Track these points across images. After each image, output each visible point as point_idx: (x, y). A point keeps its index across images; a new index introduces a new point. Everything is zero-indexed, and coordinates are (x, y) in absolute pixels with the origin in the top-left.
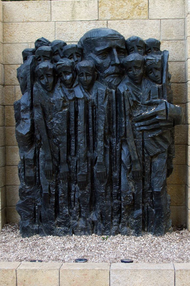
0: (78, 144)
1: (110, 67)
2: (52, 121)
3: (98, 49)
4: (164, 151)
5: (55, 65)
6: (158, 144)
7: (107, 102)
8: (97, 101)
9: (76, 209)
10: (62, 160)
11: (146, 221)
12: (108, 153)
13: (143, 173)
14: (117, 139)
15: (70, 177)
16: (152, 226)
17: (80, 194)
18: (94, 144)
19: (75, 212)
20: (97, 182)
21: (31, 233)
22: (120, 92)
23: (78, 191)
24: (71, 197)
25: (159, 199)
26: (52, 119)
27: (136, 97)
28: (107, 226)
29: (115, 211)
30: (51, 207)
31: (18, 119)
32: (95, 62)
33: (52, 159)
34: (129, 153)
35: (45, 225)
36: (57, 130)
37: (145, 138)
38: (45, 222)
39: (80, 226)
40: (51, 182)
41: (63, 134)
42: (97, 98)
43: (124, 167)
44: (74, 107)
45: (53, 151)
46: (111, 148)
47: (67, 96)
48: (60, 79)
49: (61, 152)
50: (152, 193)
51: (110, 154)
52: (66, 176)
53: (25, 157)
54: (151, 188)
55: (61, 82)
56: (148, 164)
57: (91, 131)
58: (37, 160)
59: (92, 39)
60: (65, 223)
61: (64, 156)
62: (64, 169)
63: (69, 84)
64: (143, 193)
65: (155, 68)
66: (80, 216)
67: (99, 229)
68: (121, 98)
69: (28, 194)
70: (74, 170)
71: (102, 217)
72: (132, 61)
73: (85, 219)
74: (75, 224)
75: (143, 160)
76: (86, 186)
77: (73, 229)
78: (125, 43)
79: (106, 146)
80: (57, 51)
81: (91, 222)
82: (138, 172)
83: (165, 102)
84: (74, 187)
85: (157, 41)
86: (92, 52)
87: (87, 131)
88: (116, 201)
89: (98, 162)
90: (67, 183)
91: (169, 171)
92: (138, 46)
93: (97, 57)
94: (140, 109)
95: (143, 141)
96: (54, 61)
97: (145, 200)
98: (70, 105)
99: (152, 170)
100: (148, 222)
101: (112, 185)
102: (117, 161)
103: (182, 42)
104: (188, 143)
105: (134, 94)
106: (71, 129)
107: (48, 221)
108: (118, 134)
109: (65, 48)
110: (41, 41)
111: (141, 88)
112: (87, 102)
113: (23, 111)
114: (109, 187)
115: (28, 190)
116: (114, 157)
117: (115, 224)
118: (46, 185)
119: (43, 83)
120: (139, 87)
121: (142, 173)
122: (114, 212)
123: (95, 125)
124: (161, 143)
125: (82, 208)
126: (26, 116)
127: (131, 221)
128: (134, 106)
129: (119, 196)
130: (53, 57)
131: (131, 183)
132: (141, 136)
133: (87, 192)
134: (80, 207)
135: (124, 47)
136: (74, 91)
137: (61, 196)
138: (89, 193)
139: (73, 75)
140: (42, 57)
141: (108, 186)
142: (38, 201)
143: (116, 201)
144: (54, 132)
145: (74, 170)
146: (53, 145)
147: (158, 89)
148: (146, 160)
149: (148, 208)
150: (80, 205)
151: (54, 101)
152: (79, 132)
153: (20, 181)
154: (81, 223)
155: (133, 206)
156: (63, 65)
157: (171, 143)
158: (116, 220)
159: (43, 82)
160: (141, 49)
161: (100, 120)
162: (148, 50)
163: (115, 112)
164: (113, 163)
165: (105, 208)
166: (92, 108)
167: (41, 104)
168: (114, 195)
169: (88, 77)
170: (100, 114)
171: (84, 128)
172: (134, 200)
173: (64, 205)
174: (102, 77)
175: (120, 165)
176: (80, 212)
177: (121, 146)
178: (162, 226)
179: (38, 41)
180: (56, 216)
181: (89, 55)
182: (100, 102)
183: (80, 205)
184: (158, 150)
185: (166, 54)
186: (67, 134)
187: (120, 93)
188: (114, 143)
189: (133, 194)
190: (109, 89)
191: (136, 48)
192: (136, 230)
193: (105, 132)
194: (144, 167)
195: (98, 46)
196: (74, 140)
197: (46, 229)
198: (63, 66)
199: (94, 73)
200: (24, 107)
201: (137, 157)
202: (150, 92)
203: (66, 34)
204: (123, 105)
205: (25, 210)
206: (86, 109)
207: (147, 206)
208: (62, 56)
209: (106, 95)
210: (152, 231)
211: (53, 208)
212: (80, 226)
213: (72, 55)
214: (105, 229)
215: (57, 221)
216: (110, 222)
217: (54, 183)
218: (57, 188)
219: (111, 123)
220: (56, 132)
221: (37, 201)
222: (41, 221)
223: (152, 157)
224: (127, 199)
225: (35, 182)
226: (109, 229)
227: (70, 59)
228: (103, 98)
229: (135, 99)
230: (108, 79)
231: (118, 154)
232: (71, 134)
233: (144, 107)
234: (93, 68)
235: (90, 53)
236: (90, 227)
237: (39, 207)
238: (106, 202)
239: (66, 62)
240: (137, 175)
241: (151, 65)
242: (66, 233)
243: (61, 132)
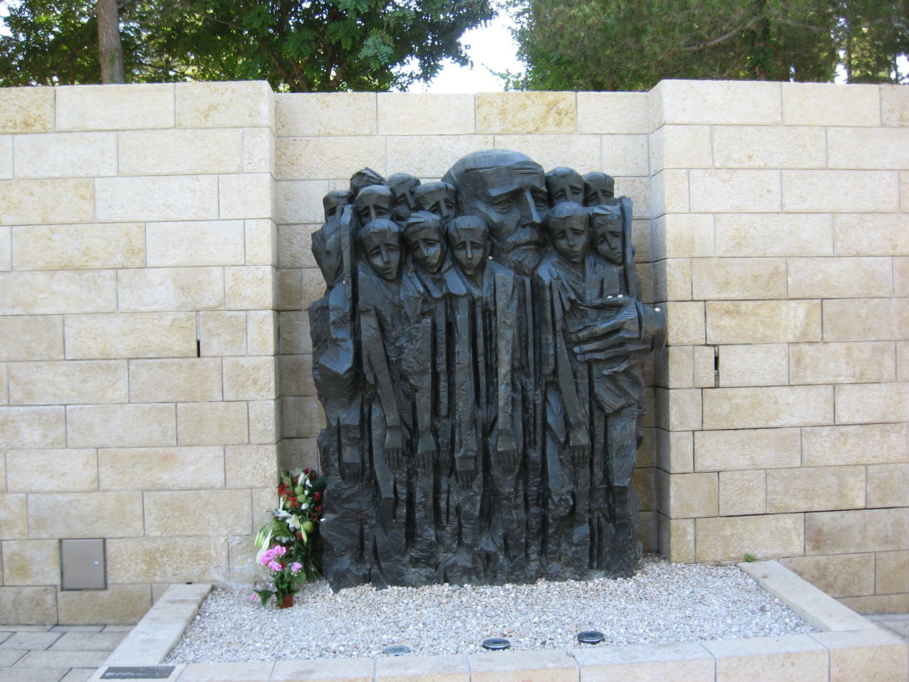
3: (494, 192)
6: (621, 389)
7: (515, 302)
20: (496, 472)
22: (543, 282)
38: (386, 560)
43: (552, 437)
46: (524, 399)
49: (419, 409)
52: (431, 459)
57: (482, 366)
60: (429, 558)
61: (425, 418)
62: (425, 445)
63: (432, 266)
64: (590, 489)
74: (451, 561)
79: (515, 396)
81: (484, 555)
111: (584, 273)
113: (333, 323)
117: (534, 556)
126: (343, 334)
132: (586, 373)
136: (444, 280)
137: (421, 503)
154: (463, 559)
155: (572, 518)
159: (378, 261)
164: (529, 431)
167: (376, 309)
175: (544, 435)
182: (500, 305)
184: (622, 402)
194: (592, 436)
195: (493, 187)
198: (423, 229)
204: (549, 308)
207: (599, 518)
213: (437, 204)
217: (404, 475)
220: (409, 367)
225: (363, 474)
226: (523, 568)
227: (434, 212)
229: (573, 297)
237: (372, 527)
242: (430, 581)
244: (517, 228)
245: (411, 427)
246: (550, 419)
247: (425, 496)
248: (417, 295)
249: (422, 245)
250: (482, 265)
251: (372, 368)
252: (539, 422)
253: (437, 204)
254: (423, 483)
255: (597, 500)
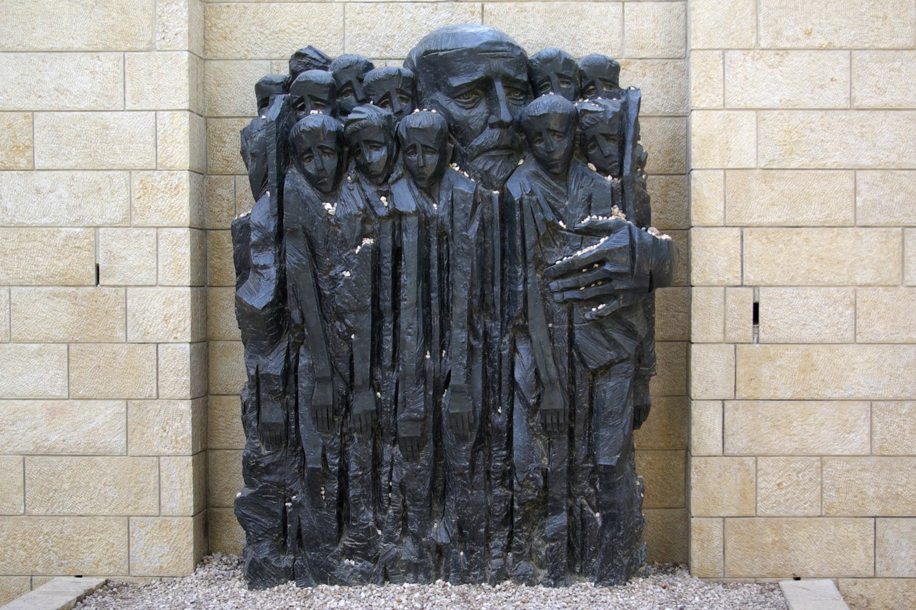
0: (402, 336)
1: (488, 130)
2: (332, 273)
3: (456, 82)
4: (625, 356)
5: (343, 122)
6: (610, 340)
7: (476, 224)
8: (452, 222)
9: (394, 513)
10: (358, 381)
11: (578, 546)
12: (480, 359)
13: (570, 416)
14: (502, 323)
15: (379, 425)
16: (594, 560)
17: (404, 472)
18: (442, 336)
19: (390, 521)
20: (449, 439)
21: (274, 576)
22: (513, 198)
23: (400, 463)
24: (380, 479)
25: (608, 487)
26: (332, 267)
27: (554, 210)
28: (476, 559)
29: (497, 519)
30: (328, 506)
31: (244, 268)
32: (448, 115)
33: (332, 376)
34: (535, 362)
35: (310, 555)
36: (346, 297)
37: (575, 320)
38: (311, 549)
39: (403, 558)
40: (328, 438)
41: (361, 310)
42: (451, 214)
44: (390, 237)
45: (334, 355)
46: (488, 347)
47: (372, 207)
48: (356, 160)
50: (595, 470)
51: (484, 364)
52: (369, 422)
54: (591, 455)
55: (356, 168)
56: (584, 392)
57: (435, 303)
58: (292, 378)
59: (441, 54)
60: (365, 549)
61: (362, 368)
62: (362, 403)
63: (377, 176)
64: (569, 468)
65: (604, 135)
66: (405, 532)
67: (455, 567)
68: (515, 214)
69: (267, 470)
70: (391, 407)
71: (465, 533)
72: (544, 115)
73: (416, 538)
75: (572, 381)
76: (420, 450)
77: (386, 566)
78: (528, 66)
79: (474, 343)
80: (349, 83)
81: (434, 548)
82: (557, 412)
83: (629, 225)
84: (390, 451)
85: (611, 61)
86: (440, 90)
87: (426, 303)
88: (498, 492)
89: (454, 386)
90: (370, 443)
91: (640, 415)
92: (560, 76)
93: (453, 104)
94: (565, 245)
95: (571, 331)
96: (339, 112)
97: (576, 489)
98: (379, 230)
99: (595, 408)
100: (582, 549)
101: (490, 449)
102: (503, 383)
103: (679, 63)
104: (690, 337)
105: (549, 203)
106: (382, 297)
107: (318, 544)
108: (507, 311)
109: (369, 77)
110: (305, 55)
111: (567, 187)
112: (425, 221)
113: (255, 245)
114: (481, 453)
115: (267, 461)
116: (494, 373)
117: (496, 552)
118: (316, 446)
119: (310, 171)
120: (560, 186)
121: (568, 414)
122: (495, 522)
123: (445, 285)
124: (616, 336)
125: (409, 511)
126: (265, 258)
127: (539, 546)
128: (548, 236)
129: (507, 475)
130: (338, 100)
131: (539, 442)
132: (565, 317)
133: (422, 465)
134: (405, 507)
135: (524, 78)
136: (392, 194)
137: (356, 477)
138: (428, 470)
139: (390, 151)
140: (307, 99)
141: (479, 450)
142: (295, 490)
143: (498, 492)
144: (339, 304)
145: (391, 407)
146: (334, 337)
147: (610, 192)
148: (578, 382)
149: (582, 511)
150: (404, 501)
151: (338, 219)
152: (402, 303)
153: (247, 437)
154: (407, 550)
155: (545, 505)
156: (363, 122)
157: (644, 336)
158: (499, 541)
159: (310, 168)
160: (567, 83)
161: (459, 273)
162: (587, 87)
163: (498, 251)
164: (493, 388)
165: (469, 510)
166: (439, 240)
168: (494, 473)
169: (428, 156)
170: (458, 255)
171: (417, 293)
172: (545, 488)
173: (362, 500)
174: (465, 155)
175: (512, 394)
176: (405, 519)
177: (513, 342)
178: (620, 561)
179: (299, 55)
180: (340, 531)
181: (433, 97)
182: (458, 225)
183: (404, 501)
184: (611, 355)
185: (634, 98)
186: (373, 308)
187: (513, 203)
188: (496, 333)
189: (545, 475)
190: (483, 189)
191: (555, 79)
192: (553, 570)
193: (470, 303)
194: (572, 399)
195: (455, 74)
196: (391, 326)
197: (315, 566)
198: (364, 127)
199: (444, 145)
200: (259, 234)
201: (553, 371)
202: (590, 199)
203: (373, 37)
204: (518, 232)
205: (258, 514)
206: (424, 242)
208: (360, 98)
209: (475, 204)
210: (593, 574)
211: (333, 508)
212: (403, 558)
213: (388, 95)
214: (470, 568)
216: (482, 548)
217: (337, 440)
218: (343, 454)
219: (489, 279)
220: (344, 303)
221: (291, 490)
222: (301, 545)
223: (594, 373)
224: (528, 486)
225: (287, 438)
226: (482, 567)
227: (383, 106)
228: (467, 215)
229: (550, 217)
230: (481, 163)
231: (505, 363)
232: (382, 308)
233: (575, 240)
234: (441, 131)
235: (434, 92)
236: (430, 560)
238: (472, 494)
239: (368, 113)
240: (555, 421)
241: (592, 125)
242: (366, 578)
243: (356, 304)
244: (483, 129)
245: (348, 380)
246: (518, 375)
247: (361, 469)
248: (356, 211)
249: (364, 148)
250: (440, 173)
251: (298, 302)
252: (505, 378)
253: (388, 95)
254: (359, 451)
255: (580, 482)
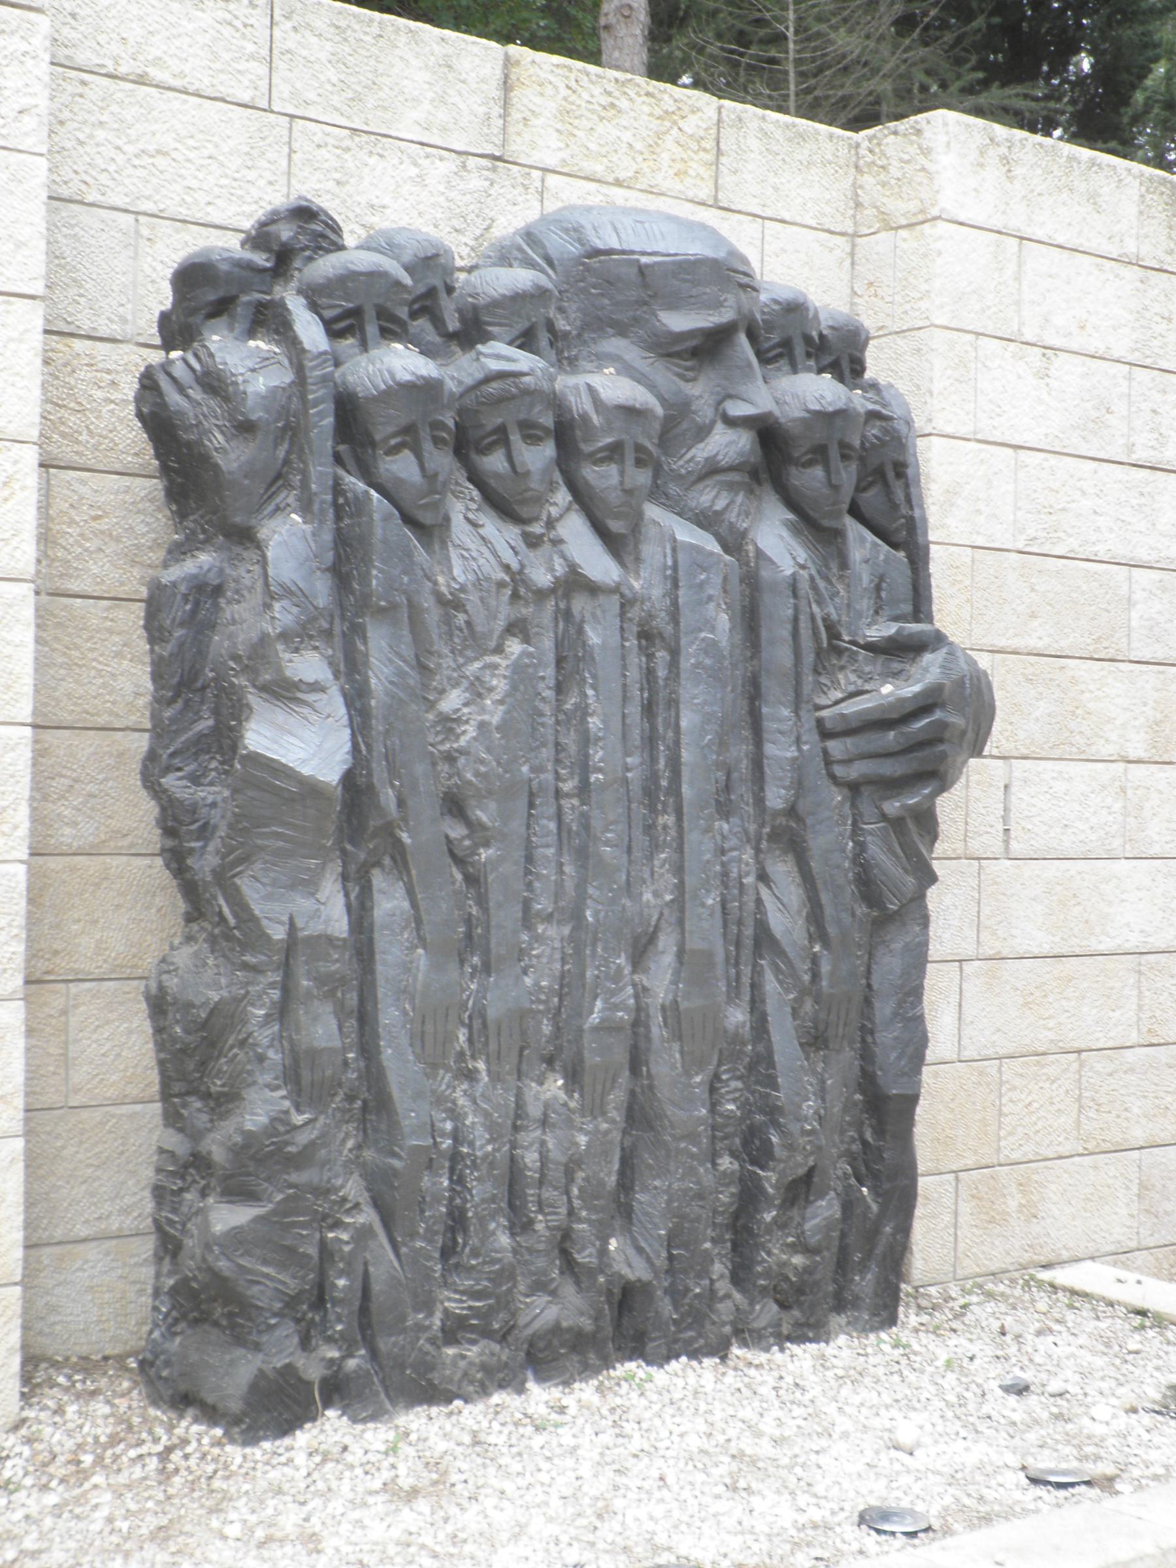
30: (427, 1230)
36: (482, 762)
43: (777, 970)
53: (300, 923)
215: (446, 1311)
237: (363, 1234)
